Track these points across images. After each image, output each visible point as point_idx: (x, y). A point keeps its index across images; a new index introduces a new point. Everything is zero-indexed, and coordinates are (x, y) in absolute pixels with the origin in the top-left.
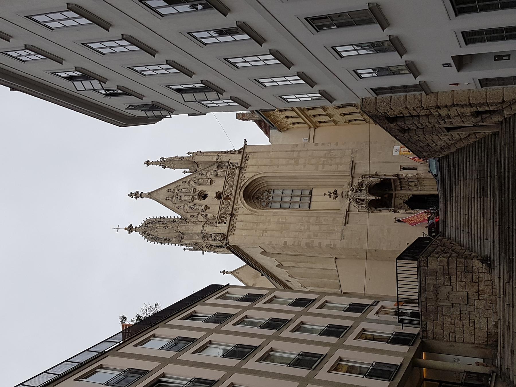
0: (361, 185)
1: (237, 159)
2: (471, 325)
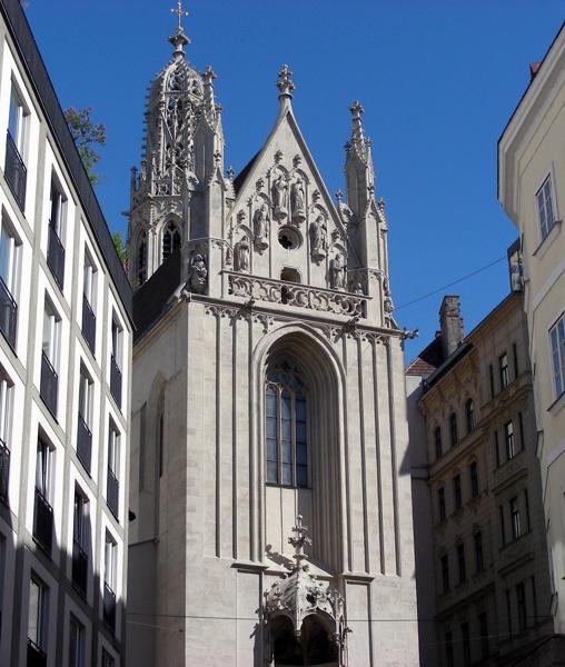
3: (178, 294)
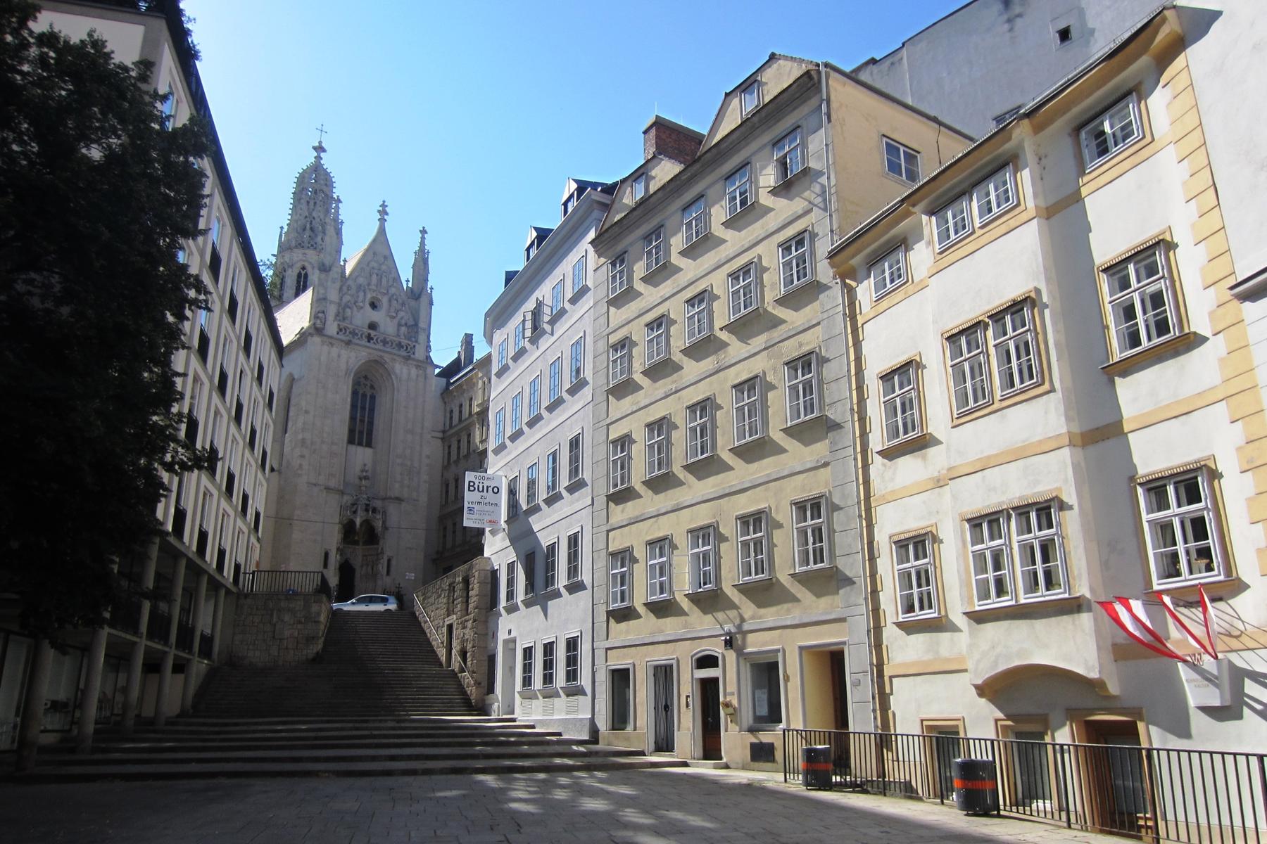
0: (374, 510)
1: (419, 354)
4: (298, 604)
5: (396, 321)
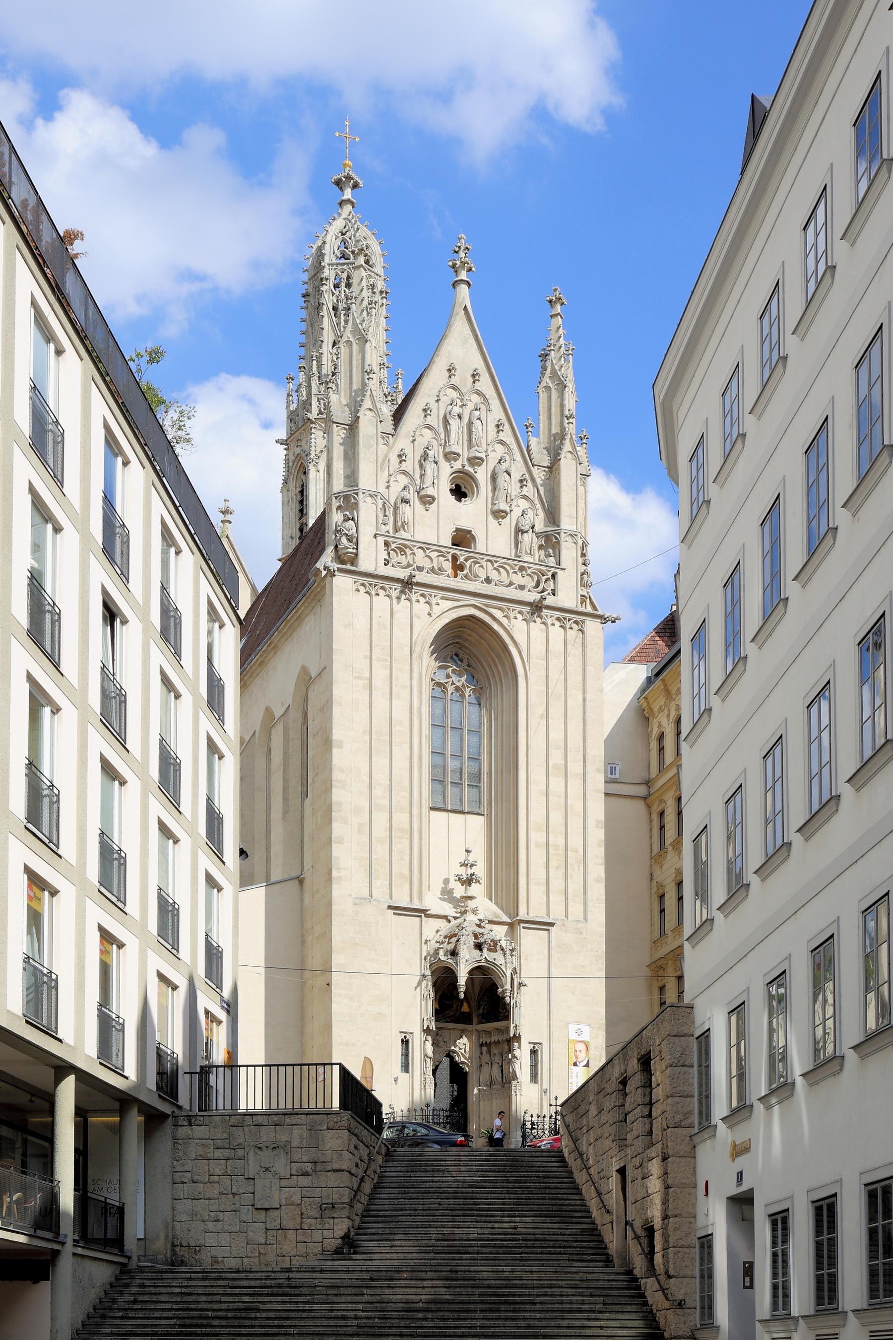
2: (212, 1214)
3: (320, 565)
4: (297, 1135)
5: (509, 523)
